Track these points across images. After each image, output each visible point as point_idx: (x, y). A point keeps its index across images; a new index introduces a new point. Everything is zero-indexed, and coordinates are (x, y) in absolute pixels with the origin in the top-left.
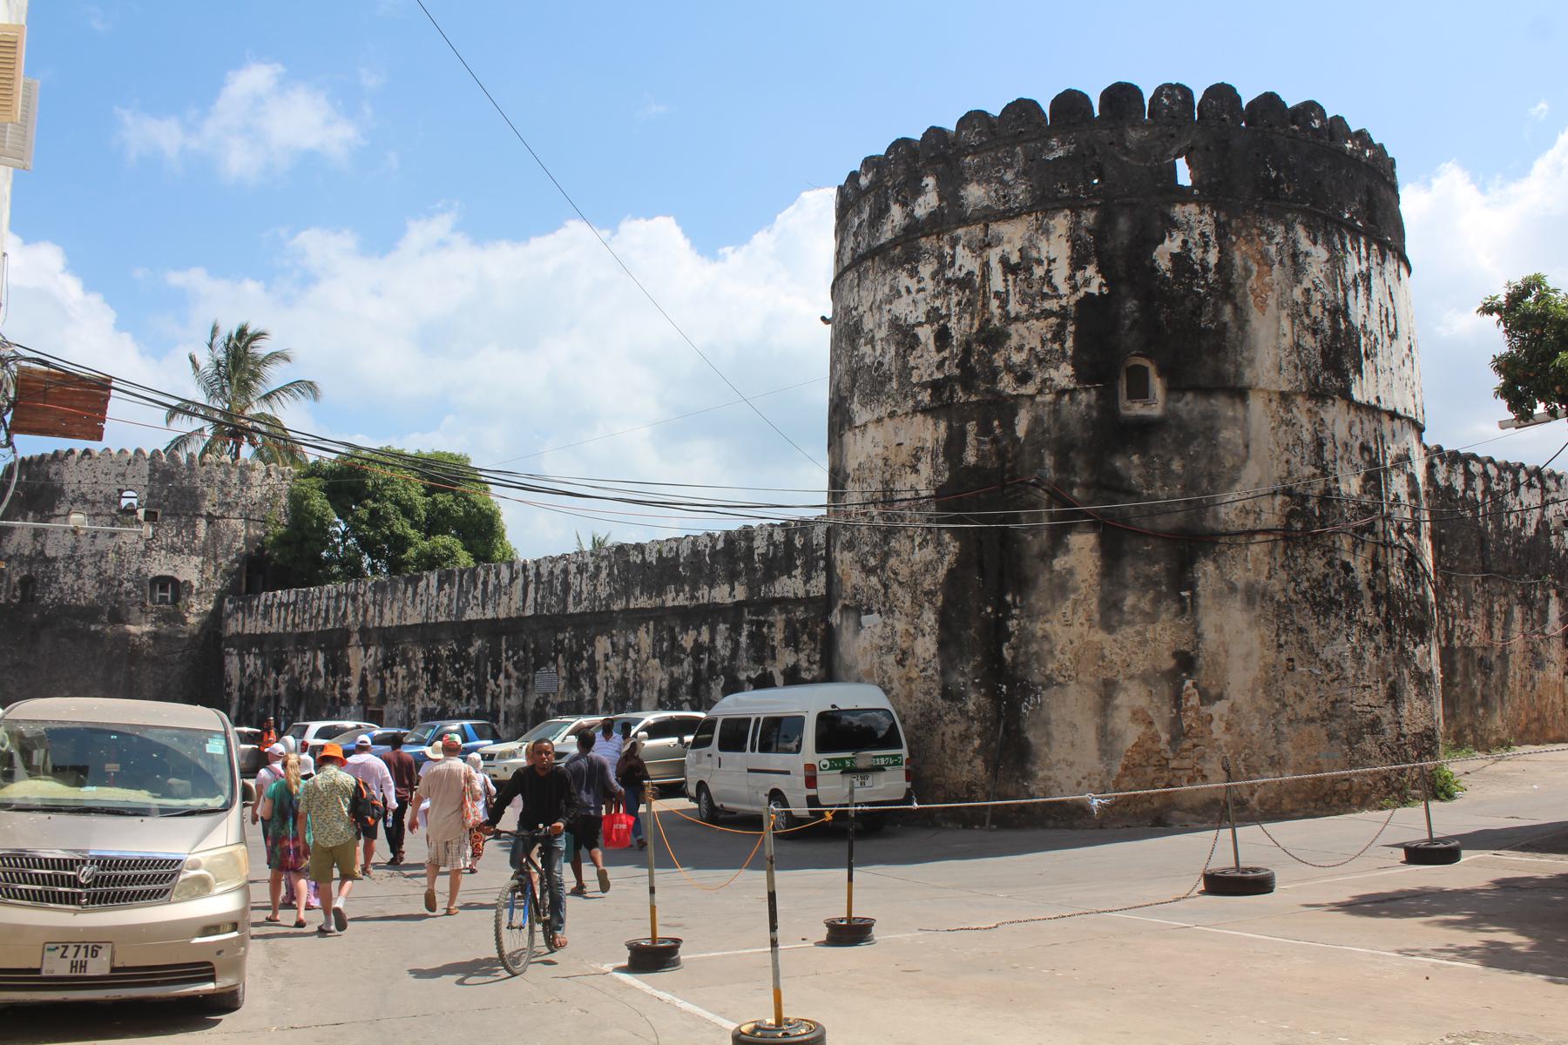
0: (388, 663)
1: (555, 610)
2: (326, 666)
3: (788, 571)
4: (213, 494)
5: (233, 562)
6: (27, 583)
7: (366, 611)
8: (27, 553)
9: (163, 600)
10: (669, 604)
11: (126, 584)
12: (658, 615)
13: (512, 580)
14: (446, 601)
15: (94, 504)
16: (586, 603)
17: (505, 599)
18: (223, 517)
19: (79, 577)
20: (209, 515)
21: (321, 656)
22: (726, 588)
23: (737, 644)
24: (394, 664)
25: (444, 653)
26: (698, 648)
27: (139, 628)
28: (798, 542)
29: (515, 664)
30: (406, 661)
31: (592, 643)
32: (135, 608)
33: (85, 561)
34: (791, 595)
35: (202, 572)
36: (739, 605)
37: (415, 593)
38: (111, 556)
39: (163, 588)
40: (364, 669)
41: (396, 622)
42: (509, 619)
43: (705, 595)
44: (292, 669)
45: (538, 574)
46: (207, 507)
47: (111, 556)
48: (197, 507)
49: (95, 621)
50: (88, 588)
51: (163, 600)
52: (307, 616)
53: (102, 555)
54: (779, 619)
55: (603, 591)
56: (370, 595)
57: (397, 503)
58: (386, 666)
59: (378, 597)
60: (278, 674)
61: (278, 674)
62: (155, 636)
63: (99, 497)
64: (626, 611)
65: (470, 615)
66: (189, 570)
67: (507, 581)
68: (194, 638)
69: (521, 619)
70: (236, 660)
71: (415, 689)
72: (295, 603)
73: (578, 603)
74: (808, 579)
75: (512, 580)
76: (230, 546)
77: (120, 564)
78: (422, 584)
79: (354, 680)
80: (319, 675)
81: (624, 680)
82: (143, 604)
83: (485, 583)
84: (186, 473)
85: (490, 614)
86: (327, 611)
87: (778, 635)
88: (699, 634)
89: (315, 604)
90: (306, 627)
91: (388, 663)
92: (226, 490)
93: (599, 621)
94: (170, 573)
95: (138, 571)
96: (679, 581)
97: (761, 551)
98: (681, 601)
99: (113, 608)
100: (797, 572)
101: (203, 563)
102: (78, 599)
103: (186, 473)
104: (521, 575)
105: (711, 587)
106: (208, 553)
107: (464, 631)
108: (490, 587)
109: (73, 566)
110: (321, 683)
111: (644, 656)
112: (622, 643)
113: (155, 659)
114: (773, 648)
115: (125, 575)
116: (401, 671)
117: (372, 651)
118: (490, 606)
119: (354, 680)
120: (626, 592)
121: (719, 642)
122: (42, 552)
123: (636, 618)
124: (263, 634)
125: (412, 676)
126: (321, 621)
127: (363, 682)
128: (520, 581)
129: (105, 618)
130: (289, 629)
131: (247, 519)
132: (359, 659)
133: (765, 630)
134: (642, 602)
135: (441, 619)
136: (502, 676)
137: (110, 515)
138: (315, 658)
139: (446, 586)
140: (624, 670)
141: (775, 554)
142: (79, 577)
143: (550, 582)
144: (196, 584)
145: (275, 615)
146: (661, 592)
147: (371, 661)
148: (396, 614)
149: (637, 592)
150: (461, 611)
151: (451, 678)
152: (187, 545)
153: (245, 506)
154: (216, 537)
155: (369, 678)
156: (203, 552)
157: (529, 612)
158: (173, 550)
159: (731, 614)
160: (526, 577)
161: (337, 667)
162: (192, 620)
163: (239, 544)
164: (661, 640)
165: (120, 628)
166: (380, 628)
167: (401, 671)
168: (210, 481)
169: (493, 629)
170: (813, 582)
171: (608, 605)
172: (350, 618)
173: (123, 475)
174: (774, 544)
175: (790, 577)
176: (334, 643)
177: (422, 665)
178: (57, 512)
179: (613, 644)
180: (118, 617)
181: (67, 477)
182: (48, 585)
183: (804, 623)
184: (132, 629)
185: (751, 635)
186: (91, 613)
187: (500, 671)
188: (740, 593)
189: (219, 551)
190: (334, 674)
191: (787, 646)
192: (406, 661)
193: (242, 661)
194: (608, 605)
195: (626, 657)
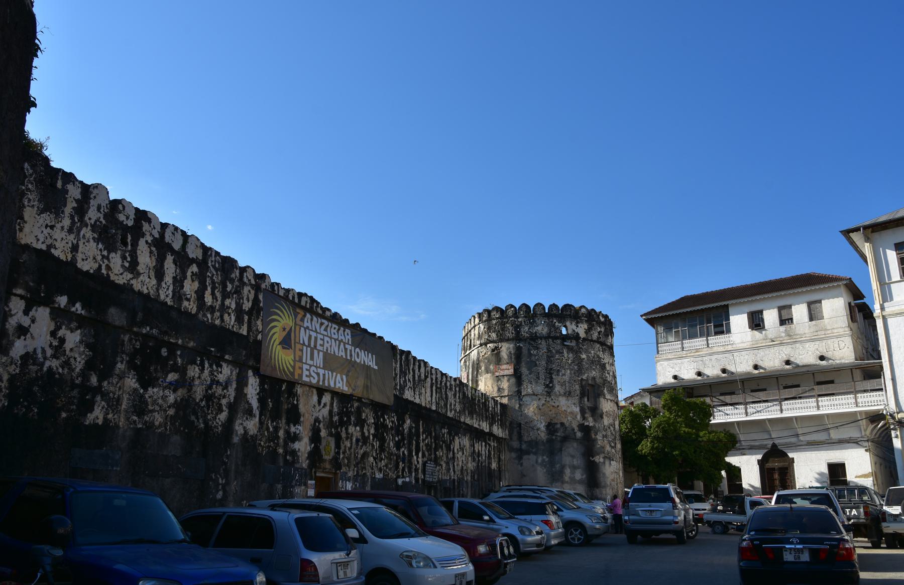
2: (262, 400)
13: (426, 377)
24: (348, 423)
40: (317, 420)
60: (146, 382)
61: (146, 382)
71: (365, 455)
75: (426, 377)
79: (303, 430)
90: (230, 320)
119: (303, 430)
127: (315, 438)
147: (325, 412)
155: (323, 433)
167: (355, 431)
190: (275, 416)
192: (361, 423)
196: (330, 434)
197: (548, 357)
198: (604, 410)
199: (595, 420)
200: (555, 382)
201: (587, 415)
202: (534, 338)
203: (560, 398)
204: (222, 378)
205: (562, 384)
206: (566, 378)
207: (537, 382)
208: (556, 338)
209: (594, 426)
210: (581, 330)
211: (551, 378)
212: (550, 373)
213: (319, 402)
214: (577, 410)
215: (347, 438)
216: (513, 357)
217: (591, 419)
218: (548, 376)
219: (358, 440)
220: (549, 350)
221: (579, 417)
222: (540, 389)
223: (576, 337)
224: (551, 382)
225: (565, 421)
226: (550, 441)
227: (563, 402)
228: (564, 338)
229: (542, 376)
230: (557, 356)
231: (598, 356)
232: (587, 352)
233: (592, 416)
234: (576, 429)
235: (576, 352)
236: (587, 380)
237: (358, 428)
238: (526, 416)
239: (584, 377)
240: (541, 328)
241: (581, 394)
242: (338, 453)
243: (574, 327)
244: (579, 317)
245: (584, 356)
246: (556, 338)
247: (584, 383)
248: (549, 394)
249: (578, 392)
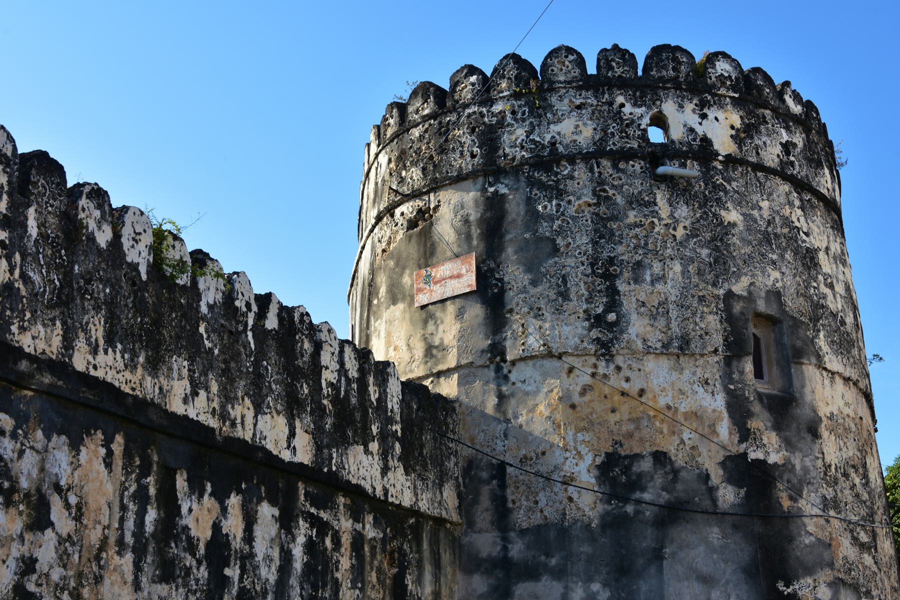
23: (286, 556)
26: (219, 542)
98: (199, 410)
100: (374, 446)
111: (94, 536)
140: (28, 565)
195: (40, 521)
197: (599, 219)
198: (824, 411)
199: (789, 444)
200: (628, 304)
201: (753, 424)
202: (547, 160)
203: (651, 364)
205: (659, 311)
206: (670, 290)
207: (559, 311)
208: (627, 155)
209: (787, 466)
210: (721, 128)
211: (613, 293)
212: (606, 273)
214: (718, 403)
216: (475, 232)
217: (771, 438)
218: (601, 285)
220: (601, 197)
221: (724, 429)
222: (571, 331)
223: (703, 150)
224: (613, 304)
225: (670, 446)
226: (614, 524)
227: (660, 377)
228: (656, 156)
229: (578, 287)
230: (632, 216)
231: (787, 222)
232: (741, 201)
233: (778, 427)
234: (716, 475)
235: (707, 200)
236: (750, 298)
238: (524, 437)
239: (740, 287)
240: (572, 128)
241: (727, 344)
243: (693, 120)
244: (710, 89)
245: (733, 216)
246: (627, 155)
247: (737, 308)
248: (605, 349)
249: (717, 340)
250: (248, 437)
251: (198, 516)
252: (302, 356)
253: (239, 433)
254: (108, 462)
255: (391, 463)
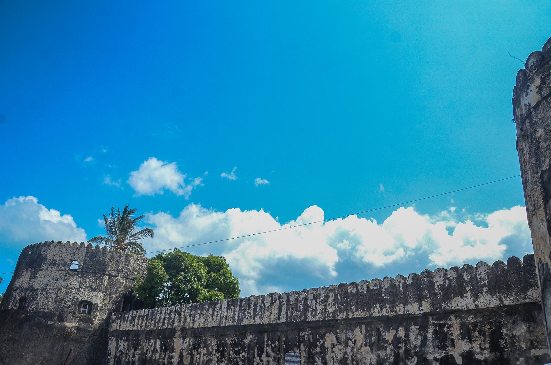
0: (196, 346)
1: (299, 319)
2: (161, 347)
3: (461, 293)
4: (113, 265)
5: (118, 297)
6: (23, 300)
7: (185, 320)
8: (25, 286)
9: (84, 312)
10: (376, 315)
11: (68, 303)
12: (368, 322)
13: (272, 303)
14: (231, 315)
15: (59, 266)
16: (319, 315)
17: (267, 313)
18: (116, 276)
19: (47, 298)
20: (110, 274)
21: (159, 342)
22: (416, 305)
23: (425, 338)
24: (199, 347)
25: (229, 342)
27: (71, 324)
28: (466, 277)
29: (272, 349)
30: (206, 346)
31: (323, 337)
32: (70, 315)
33: (51, 291)
34: (464, 308)
35: (103, 300)
36: (425, 315)
37: (214, 311)
38: (63, 289)
39: (85, 306)
40: (182, 349)
41: (202, 325)
42: (270, 324)
43: (400, 309)
44: (143, 348)
45: (288, 300)
46: (109, 271)
47: (63, 289)
48: (104, 270)
49: (51, 319)
50: (50, 303)
51: (84, 312)
52: (153, 322)
53: (59, 289)
54: (455, 323)
55: (331, 309)
56: (188, 312)
57: (195, 274)
58: (194, 348)
59: (193, 313)
60: (135, 350)
61: (135, 350)
62: (78, 329)
63: (62, 263)
64: (346, 319)
65: (246, 322)
66: (98, 299)
67: (269, 304)
68: (96, 331)
69: (277, 324)
70: (114, 343)
72: (147, 316)
73: (314, 313)
74: (476, 298)
75: (272, 303)
76: (117, 289)
77: (67, 294)
78: (218, 306)
79: (176, 355)
80: (157, 352)
81: (345, 359)
82: (75, 313)
83: (255, 306)
84: (102, 255)
85: (258, 321)
86: (164, 319)
87: (456, 332)
88: (397, 332)
89: (158, 316)
90: (152, 327)
91: (196, 346)
92: (118, 264)
93: (330, 325)
94: (89, 299)
95: (74, 297)
96: (382, 302)
97: (439, 283)
99: (60, 314)
101: (104, 296)
102: (45, 309)
103: (102, 255)
104: (278, 301)
105: (405, 305)
106: (107, 291)
107: (242, 331)
108: (259, 308)
109: (45, 293)
110: (157, 356)
111: (359, 345)
112: (343, 338)
113: (76, 340)
114: (453, 341)
115: (68, 299)
116: (203, 351)
117: (187, 340)
118: (258, 317)
119: (176, 355)
120: (347, 308)
121: (412, 337)
122: (32, 286)
123: (358, 322)
124: (129, 331)
125: (209, 353)
126: (160, 325)
127: (181, 356)
128: (277, 304)
129: (55, 318)
130: (143, 328)
131: (126, 278)
132: (179, 344)
133: (445, 329)
134: (358, 314)
135: (228, 324)
136: (264, 355)
137: (66, 271)
138: (155, 343)
139: (232, 307)
140: (345, 353)
141: (450, 285)
142: (47, 298)
143: (296, 304)
144: (100, 305)
145: (136, 322)
146: (370, 307)
147: (186, 345)
148: (202, 321)
149: (354, 308)
150: (241, 320)
151: (232, 355)
152: (98, 287)
153: (126, 272)
154: (111, 285)
155: (184, 354)
156: (105, 291)
157: (283, 320)
158: (92, 289)
159: (422, 321)
160: (281, 302)
161: (167, 348)
162: (96, 322)
163: (122, 289)
164: (371, 336)
165: (62, 324)
166: (193, 328)
167: (203, 351)
168: (112, 259)
169: (260, 330)
170: (481, 300)
171: (334, 316)
172: (176, 323)
173: (74, 254)
174: (448, 279)
175: (462, 297)
176: (166, 336)
177: (215, 348)
178: (42, 268)
179: (337, 338)
180: (61, 319)
181: (49, 253)
182: (32, 301)
183: (475, 325)
184: (68, 324)
185: (435, 332)
186: (49, 316)
187: (263, 352)
188: (426, 307)
189: (112, 291)
190: (165, 351)
191: (463, 338)
192: (206, 346)
193: (117, 343)
194: (334, 316)
195: (347, 345)
196: (189, 354)
204: (150, 344)
213: (183, 342)
215: (197, 354)
219: (204, 355)
237: (205, 349)
242: (193, 361)
250: (402, 313)
251: (389, 336)
252: (424, 283)
253: (398, 313)
254: (361, 331)
255: (480, 295)
